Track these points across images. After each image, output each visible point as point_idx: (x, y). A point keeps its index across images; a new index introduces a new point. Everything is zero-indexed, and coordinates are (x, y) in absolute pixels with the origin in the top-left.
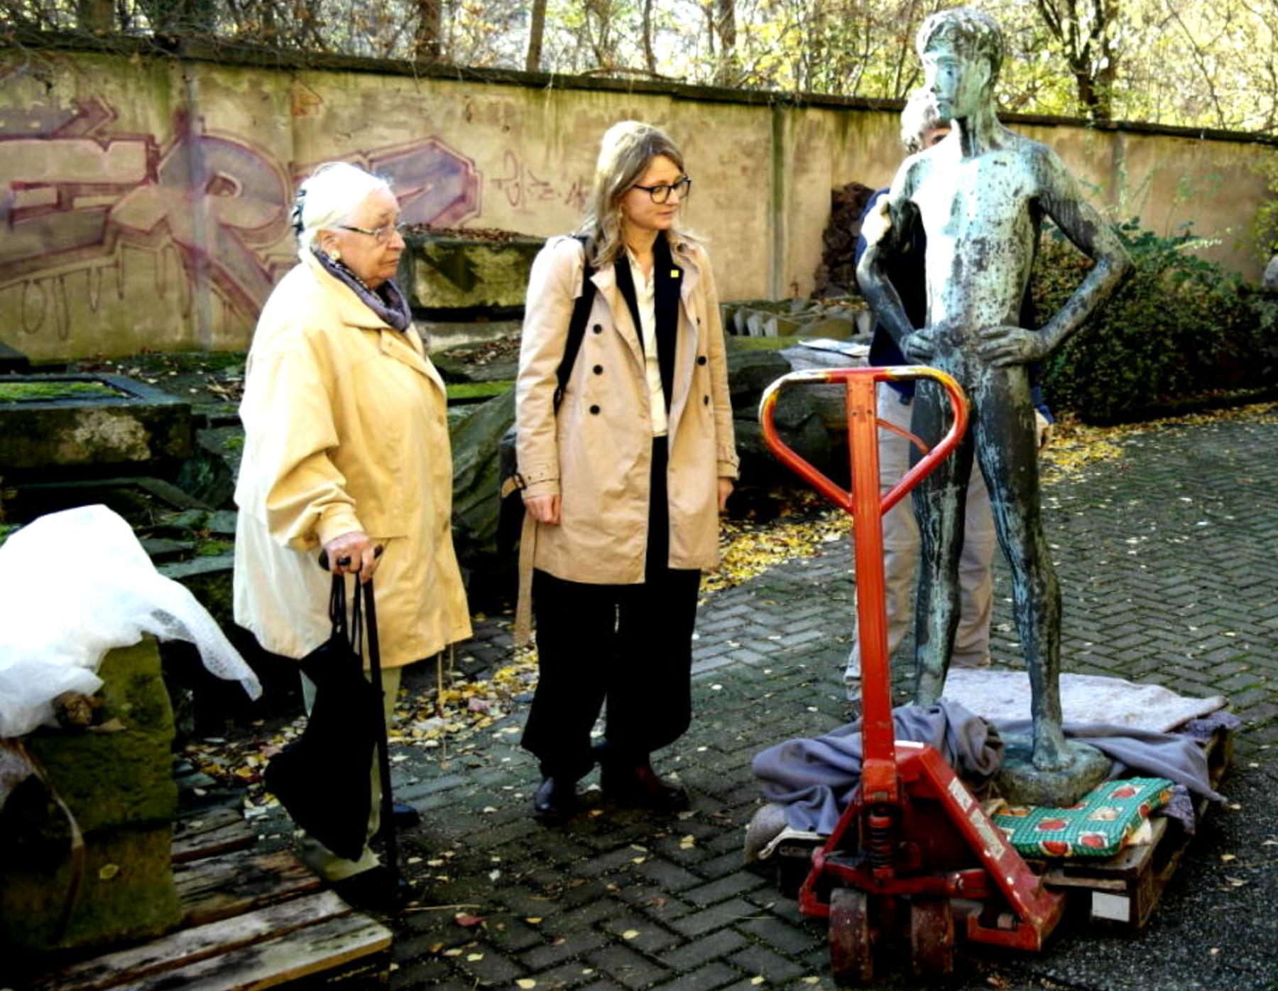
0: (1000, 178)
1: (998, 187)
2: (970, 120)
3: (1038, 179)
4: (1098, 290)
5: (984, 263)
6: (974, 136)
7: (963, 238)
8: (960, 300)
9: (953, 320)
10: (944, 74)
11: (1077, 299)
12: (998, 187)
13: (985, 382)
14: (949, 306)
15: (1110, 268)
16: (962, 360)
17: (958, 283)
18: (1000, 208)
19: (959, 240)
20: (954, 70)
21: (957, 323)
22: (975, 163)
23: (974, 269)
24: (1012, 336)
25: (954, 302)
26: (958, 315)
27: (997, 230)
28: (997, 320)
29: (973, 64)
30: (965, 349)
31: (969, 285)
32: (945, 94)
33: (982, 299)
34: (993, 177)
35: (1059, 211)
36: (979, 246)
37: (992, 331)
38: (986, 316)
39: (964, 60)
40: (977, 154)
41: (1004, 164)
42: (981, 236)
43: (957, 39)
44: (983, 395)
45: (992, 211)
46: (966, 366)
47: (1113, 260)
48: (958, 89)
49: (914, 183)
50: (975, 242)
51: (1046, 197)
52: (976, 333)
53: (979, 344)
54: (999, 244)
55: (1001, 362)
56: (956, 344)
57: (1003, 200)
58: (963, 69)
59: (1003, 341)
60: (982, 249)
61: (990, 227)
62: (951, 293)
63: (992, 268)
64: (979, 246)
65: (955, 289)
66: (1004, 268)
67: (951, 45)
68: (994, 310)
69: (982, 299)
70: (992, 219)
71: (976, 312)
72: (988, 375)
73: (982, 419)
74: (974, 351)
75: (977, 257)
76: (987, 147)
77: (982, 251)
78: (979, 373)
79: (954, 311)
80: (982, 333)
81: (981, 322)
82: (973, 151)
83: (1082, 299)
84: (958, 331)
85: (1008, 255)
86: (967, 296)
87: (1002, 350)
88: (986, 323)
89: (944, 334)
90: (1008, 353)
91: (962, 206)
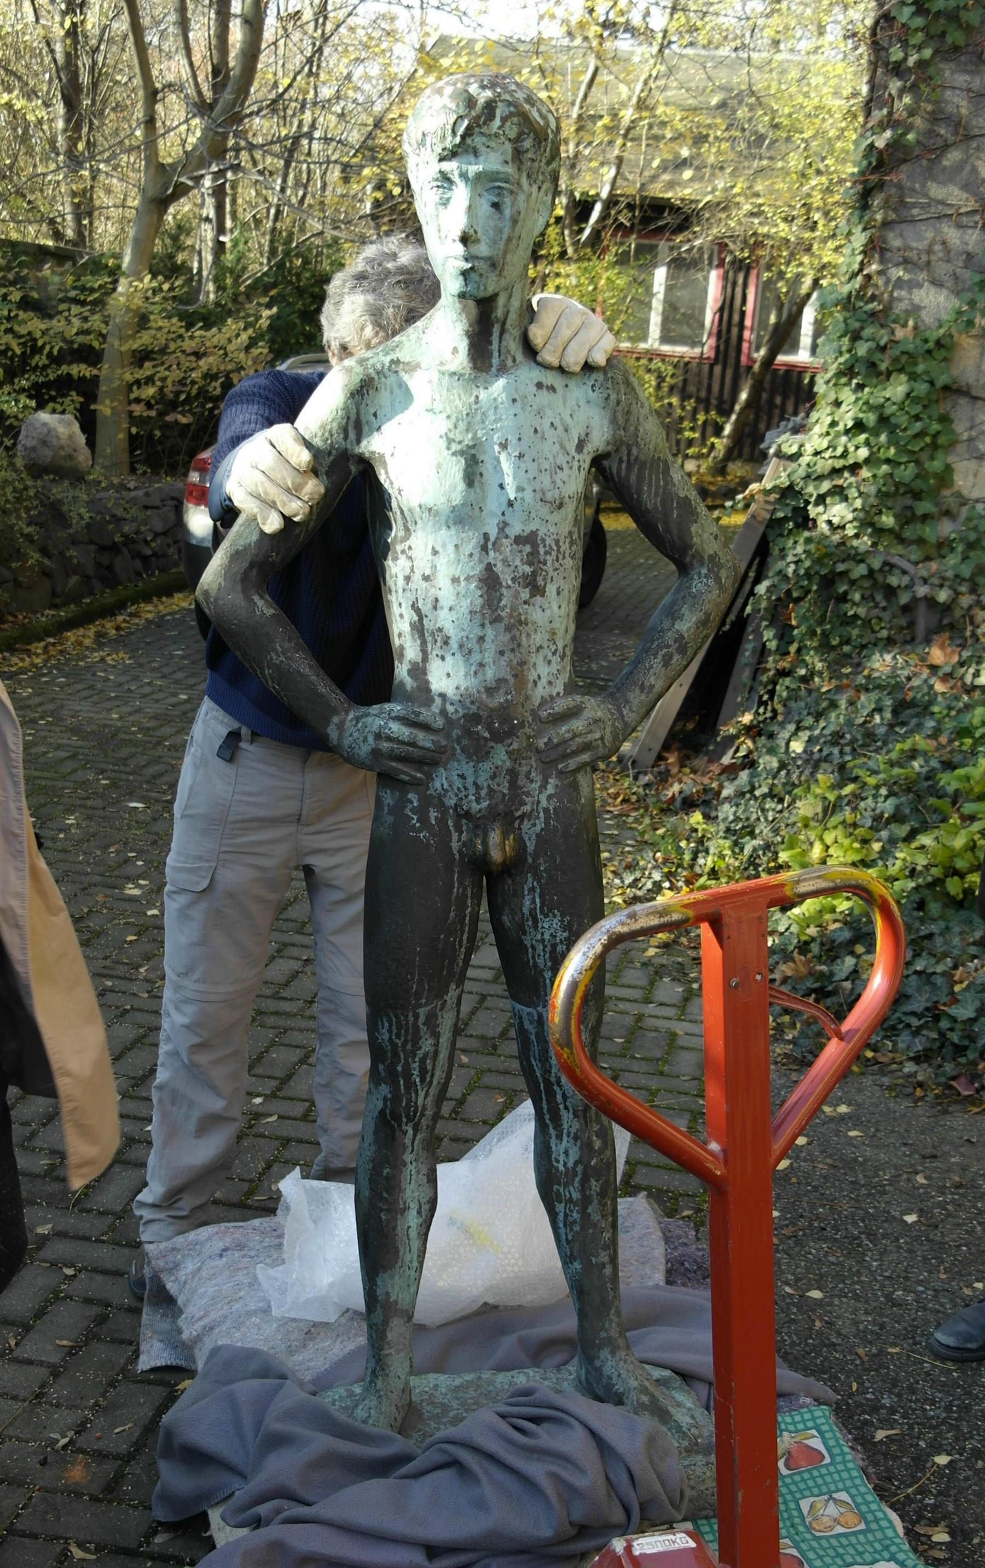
0: (549, 416)
1: (549, 433)
2: (501, 301)
3: (614, 421)
4: (704, 623)
5: (540, 582)
6: (502, 332)
7: (493, 533)
8: (502, 653)
9: (490, 691)
10: (485, 208)
11: (670, 637)
12: (549, 433)
13: (544, 803)
14: (481, 665)
15: (718, 580)
16: (508, 764)
17: (496, 620)
18: (560, 476)
19: (486, 537)
20: (508, 200)
21: (500, 699)
22: (499, 386)
23: (525, 594)
24: (588, 714)
25: (489, 657)
26: (500, 681)
27: (556, 517)
28: (559, 688)
29: (535, 188)
30: (515, 746)
31: (517, 625)
32: (483, 249)
33: (539, 648)
34: (540, 413)
35: (640, 478)
36: (528, 548)
37: (561, 705)
38: (544, 681)
39: (524, 181)
40: (503, 369)
41: (552, 389)
42: (528, 530)
43: (517, 140)
44: (540, 824)
45: (546, 480)
46: (513, 774)
47: (720, 566)
48: (509, 239)
49: (366, 416)
50: (518, 540)
51: (624, 451)
52: (534, 713)
53: (538, 734)
54: (557, 542)
55: (572, 763)
56: (498, 737)
57: (561, 460)
58: (522, 198)
59: (578, 724)
60: (534, 553)
61: (544, 510)
62: (481, 639)
63: (551, 589)
64: (528, 548)
65: (490, 632)
66: (566, 587)
67: (508, 147)
68: (554, 668)
69: (539, 648)
70: (549, 496)
71: (532, 676)
72: (550, 790)
73: (534, 869)
74: (530, 746)
75: (528, 569)
76: (520, 357)
77: (533, 558)
78: (535, 786)
79: (490, 674)
80: (544, 714)
81: (541, 691)
82: (495, 361)
83: (680, 638)
84: (504, 712)
85: (569, 562)
86: (516, 645)
87: (578, 740)
88: (545, 693)
89: (474, 718)
90: (587, 747)
91: (487, 469)
